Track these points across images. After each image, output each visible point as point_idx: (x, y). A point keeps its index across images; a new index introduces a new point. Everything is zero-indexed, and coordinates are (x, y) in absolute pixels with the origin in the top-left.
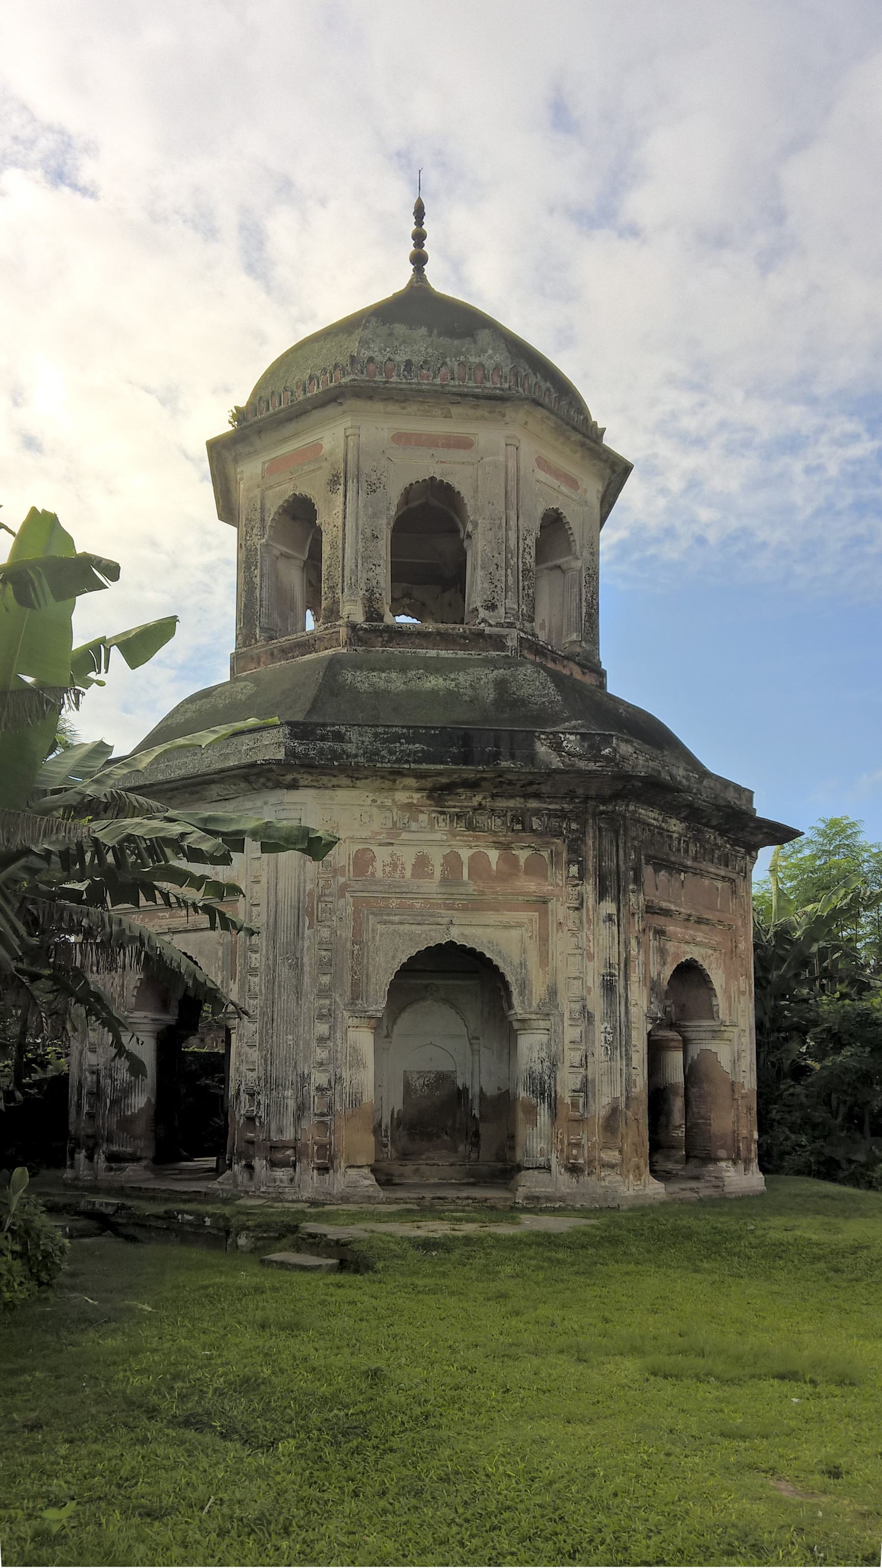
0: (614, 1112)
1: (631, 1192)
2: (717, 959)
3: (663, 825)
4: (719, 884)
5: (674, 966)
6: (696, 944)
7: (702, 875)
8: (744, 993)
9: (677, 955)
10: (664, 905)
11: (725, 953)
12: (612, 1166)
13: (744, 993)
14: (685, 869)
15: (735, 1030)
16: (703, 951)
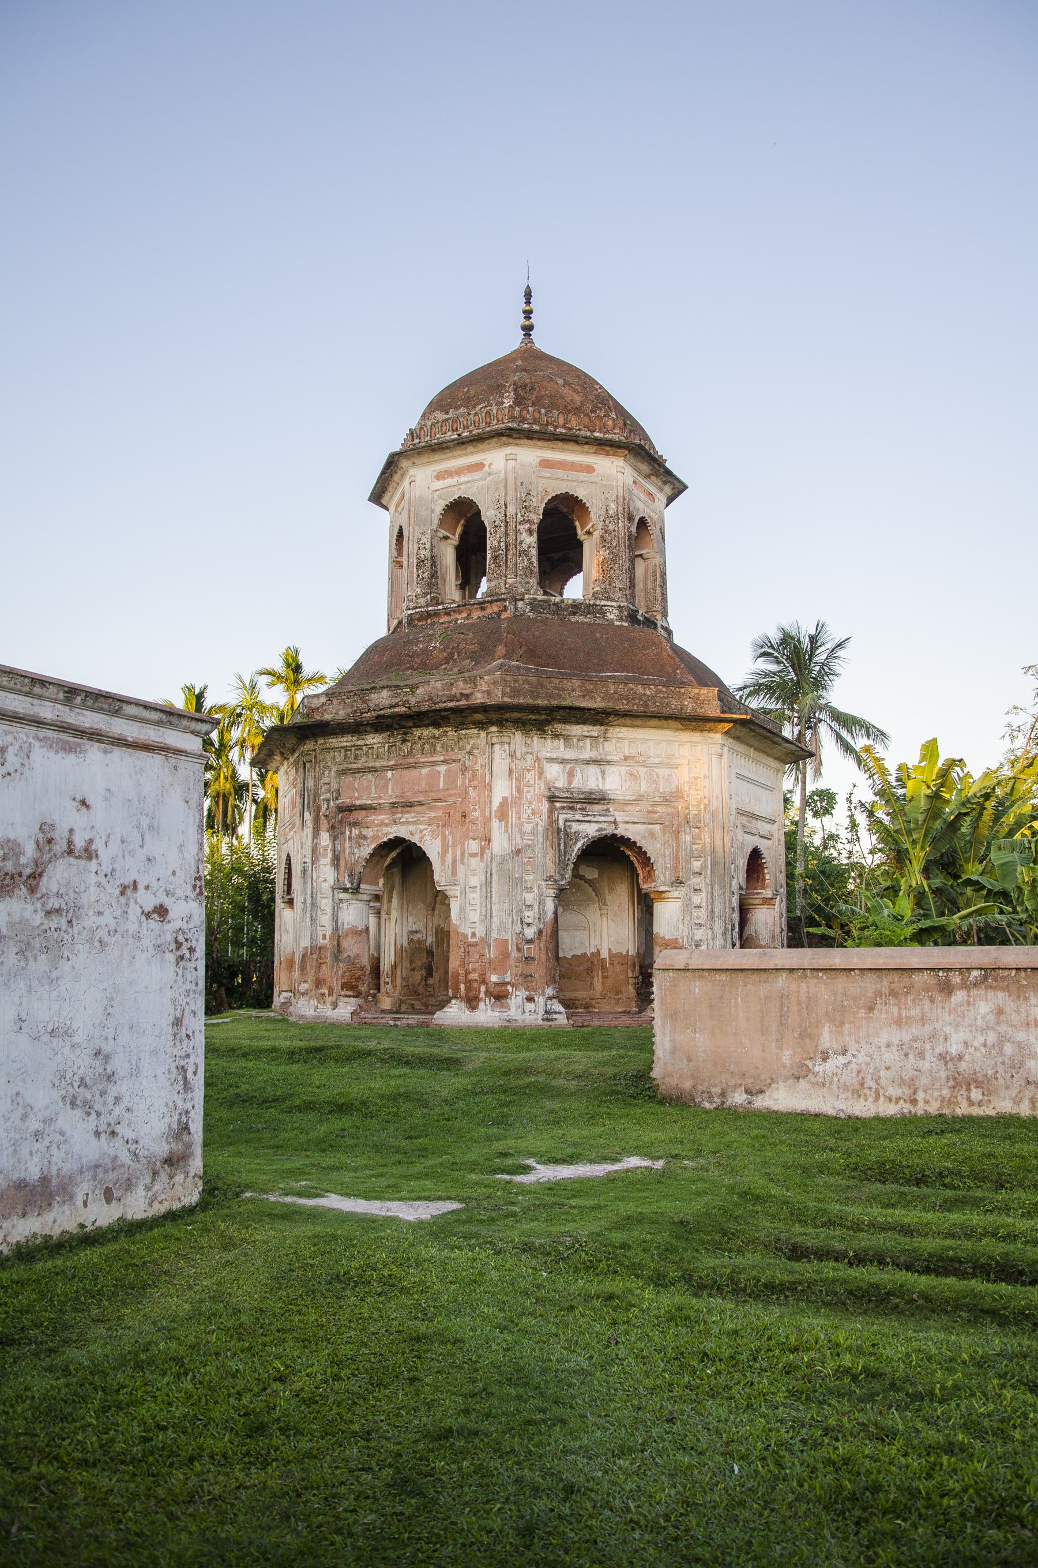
0: (304, 956)
1: (312, 1012)
2: (433, 832)
3: (359, 743)
4: (442, 769)
5: (373, 846)
6: (403, 823)
7: (414, 767)
8: (475, 855)
9: (374, 838)
10: (358, 802)
11: (444, 826)
12: (303, 994)
13: (475, 855)
14: (392, 768)
15: (458, 888)
16: (411, 828)
